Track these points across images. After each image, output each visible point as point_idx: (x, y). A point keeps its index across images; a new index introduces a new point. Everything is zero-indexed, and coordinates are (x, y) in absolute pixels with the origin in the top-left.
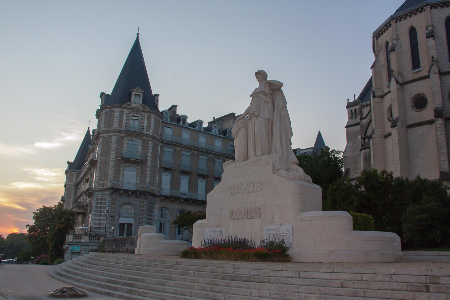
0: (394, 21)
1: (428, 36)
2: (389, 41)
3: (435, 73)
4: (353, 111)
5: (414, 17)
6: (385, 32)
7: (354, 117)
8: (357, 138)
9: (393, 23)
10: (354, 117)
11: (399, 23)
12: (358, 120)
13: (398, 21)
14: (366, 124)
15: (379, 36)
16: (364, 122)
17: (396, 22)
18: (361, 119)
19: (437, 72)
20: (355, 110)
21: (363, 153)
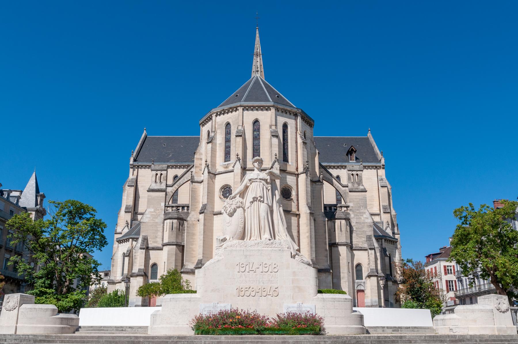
0: (242, 108)
1: (273, 134)
2: (231, 124)
3: (277, 169)
4: (159, 175)
5: (260, 112)
6: (228, 113)
7: (158, 181)
8: (160, 205)
9: (240, 109)
10: (158, 181)
11: (246, 112)
12: (163, 186)
13: (245, 109)
14: (171, 192)
15: (220, 115)
16: (169, 190)
17: (243, 109)
18: (167, 186)
19: (278, 169)
20: (161, 174)
21: (170, 223)
